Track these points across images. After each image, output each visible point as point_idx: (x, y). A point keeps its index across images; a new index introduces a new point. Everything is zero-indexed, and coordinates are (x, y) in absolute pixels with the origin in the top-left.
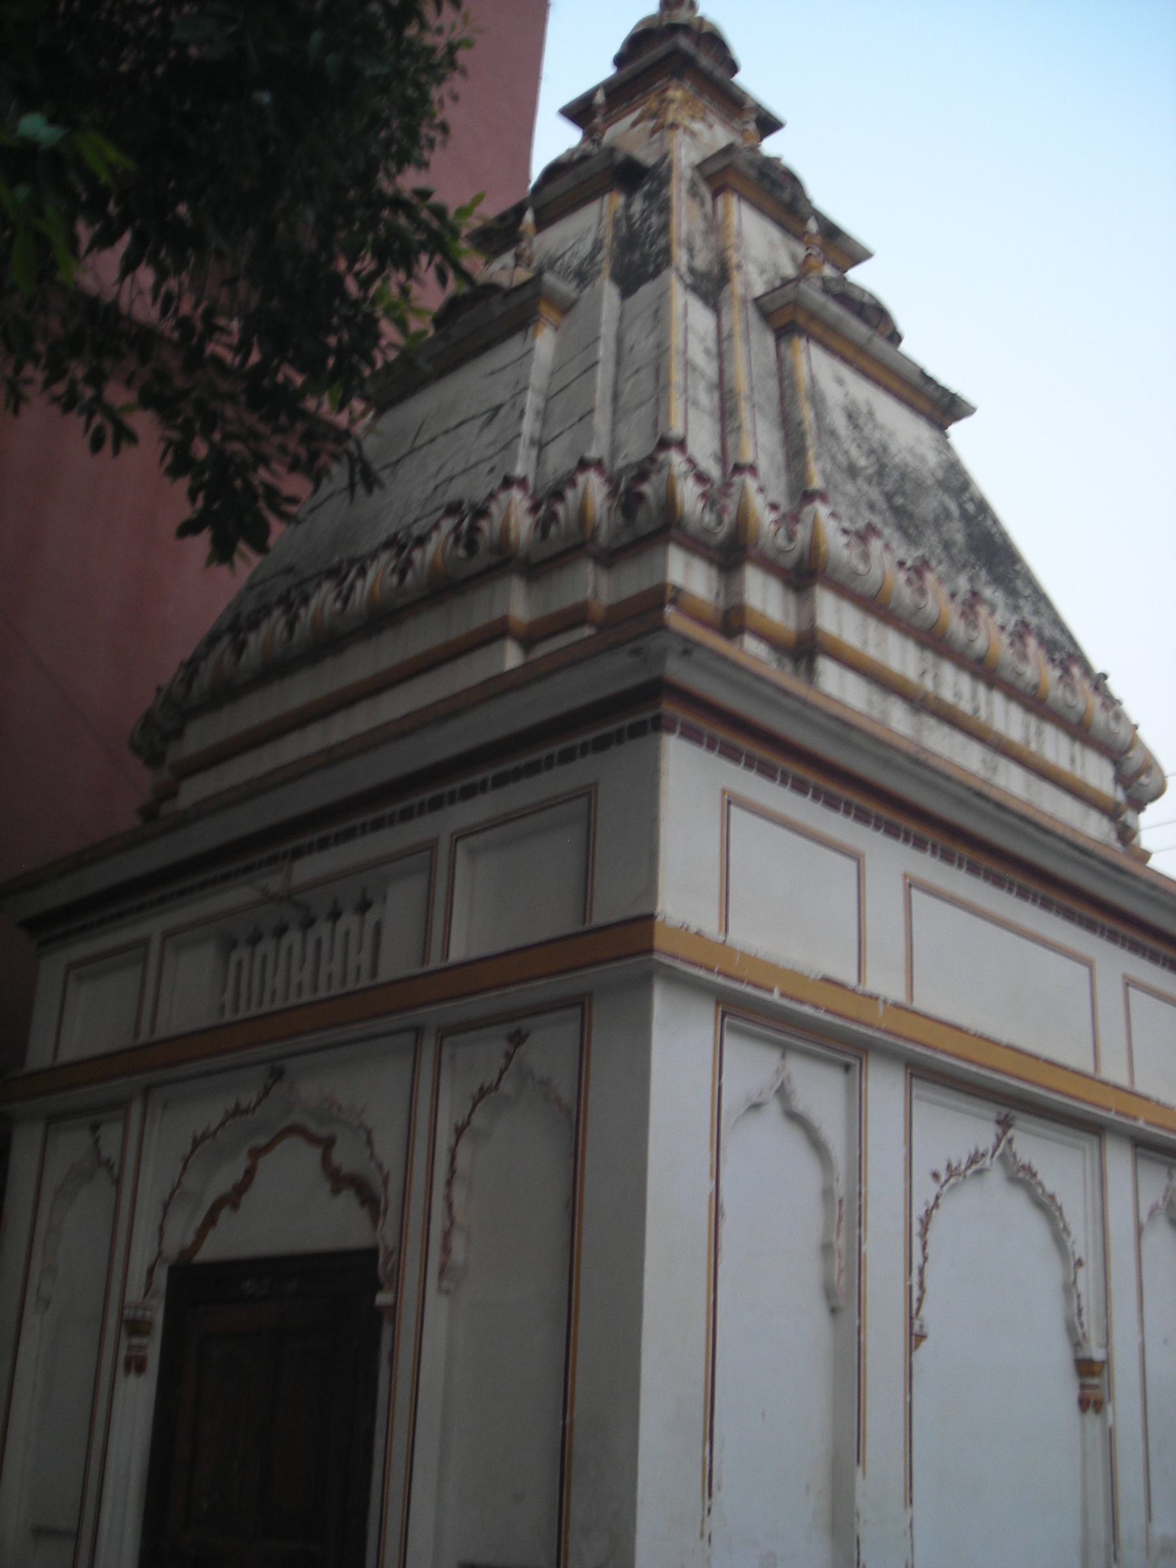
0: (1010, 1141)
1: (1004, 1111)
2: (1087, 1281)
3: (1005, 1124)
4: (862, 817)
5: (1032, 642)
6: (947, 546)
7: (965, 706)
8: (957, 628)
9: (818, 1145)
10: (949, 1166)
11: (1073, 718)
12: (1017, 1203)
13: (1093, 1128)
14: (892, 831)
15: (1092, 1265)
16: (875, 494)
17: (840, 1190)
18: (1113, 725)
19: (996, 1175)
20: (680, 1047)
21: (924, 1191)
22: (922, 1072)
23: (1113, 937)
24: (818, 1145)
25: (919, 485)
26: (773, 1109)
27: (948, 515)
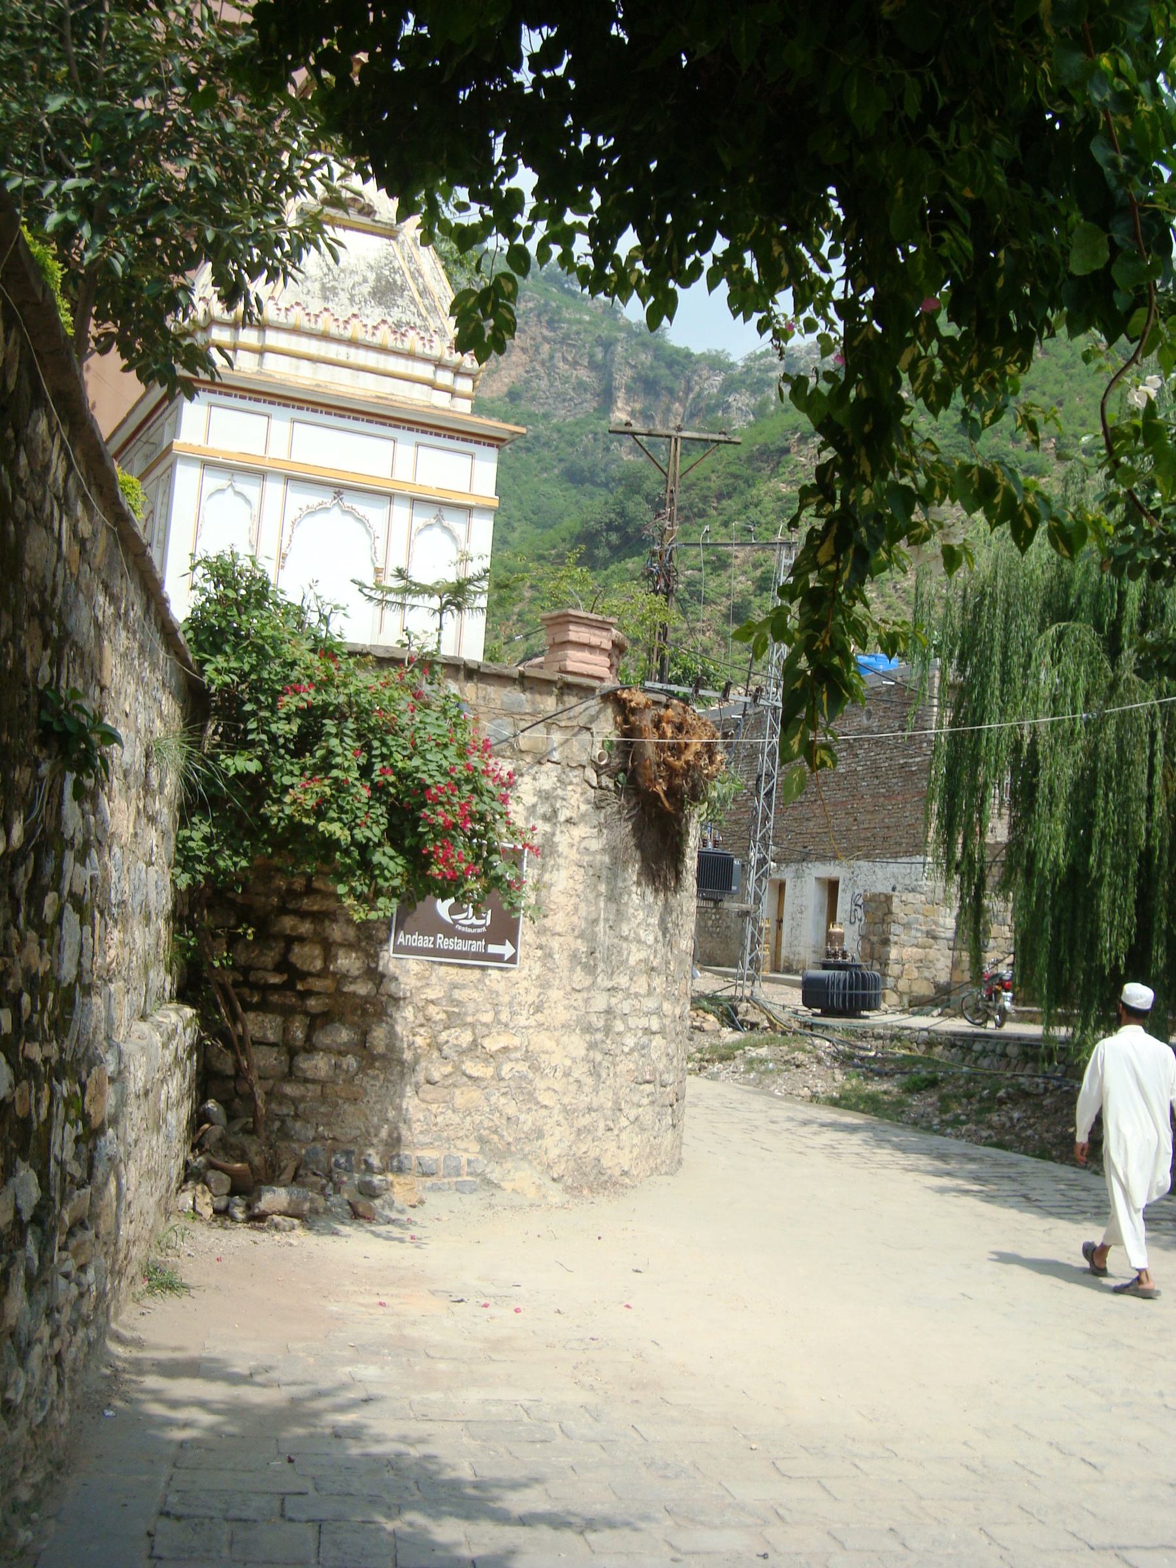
2: (380, 545)
3: (338, 494)
4: (271, 403)
5: (384, 328)
6: (352, 299)
7: (342, 358)
8: (334, 330)
9: (248, 501)
12: (349, 519)
13: (390, 496)
14: (285, 405)
15: (383, 538)
16: (317, 286)
17: (256, 512)
18: (427, 351)
19: (336, 511)
20: (186, 478)
21: (292, 513)
22: (288, 478)
24: (248, 501)
25: (352, 272)
26: (230, 491)
27: (365, 280)
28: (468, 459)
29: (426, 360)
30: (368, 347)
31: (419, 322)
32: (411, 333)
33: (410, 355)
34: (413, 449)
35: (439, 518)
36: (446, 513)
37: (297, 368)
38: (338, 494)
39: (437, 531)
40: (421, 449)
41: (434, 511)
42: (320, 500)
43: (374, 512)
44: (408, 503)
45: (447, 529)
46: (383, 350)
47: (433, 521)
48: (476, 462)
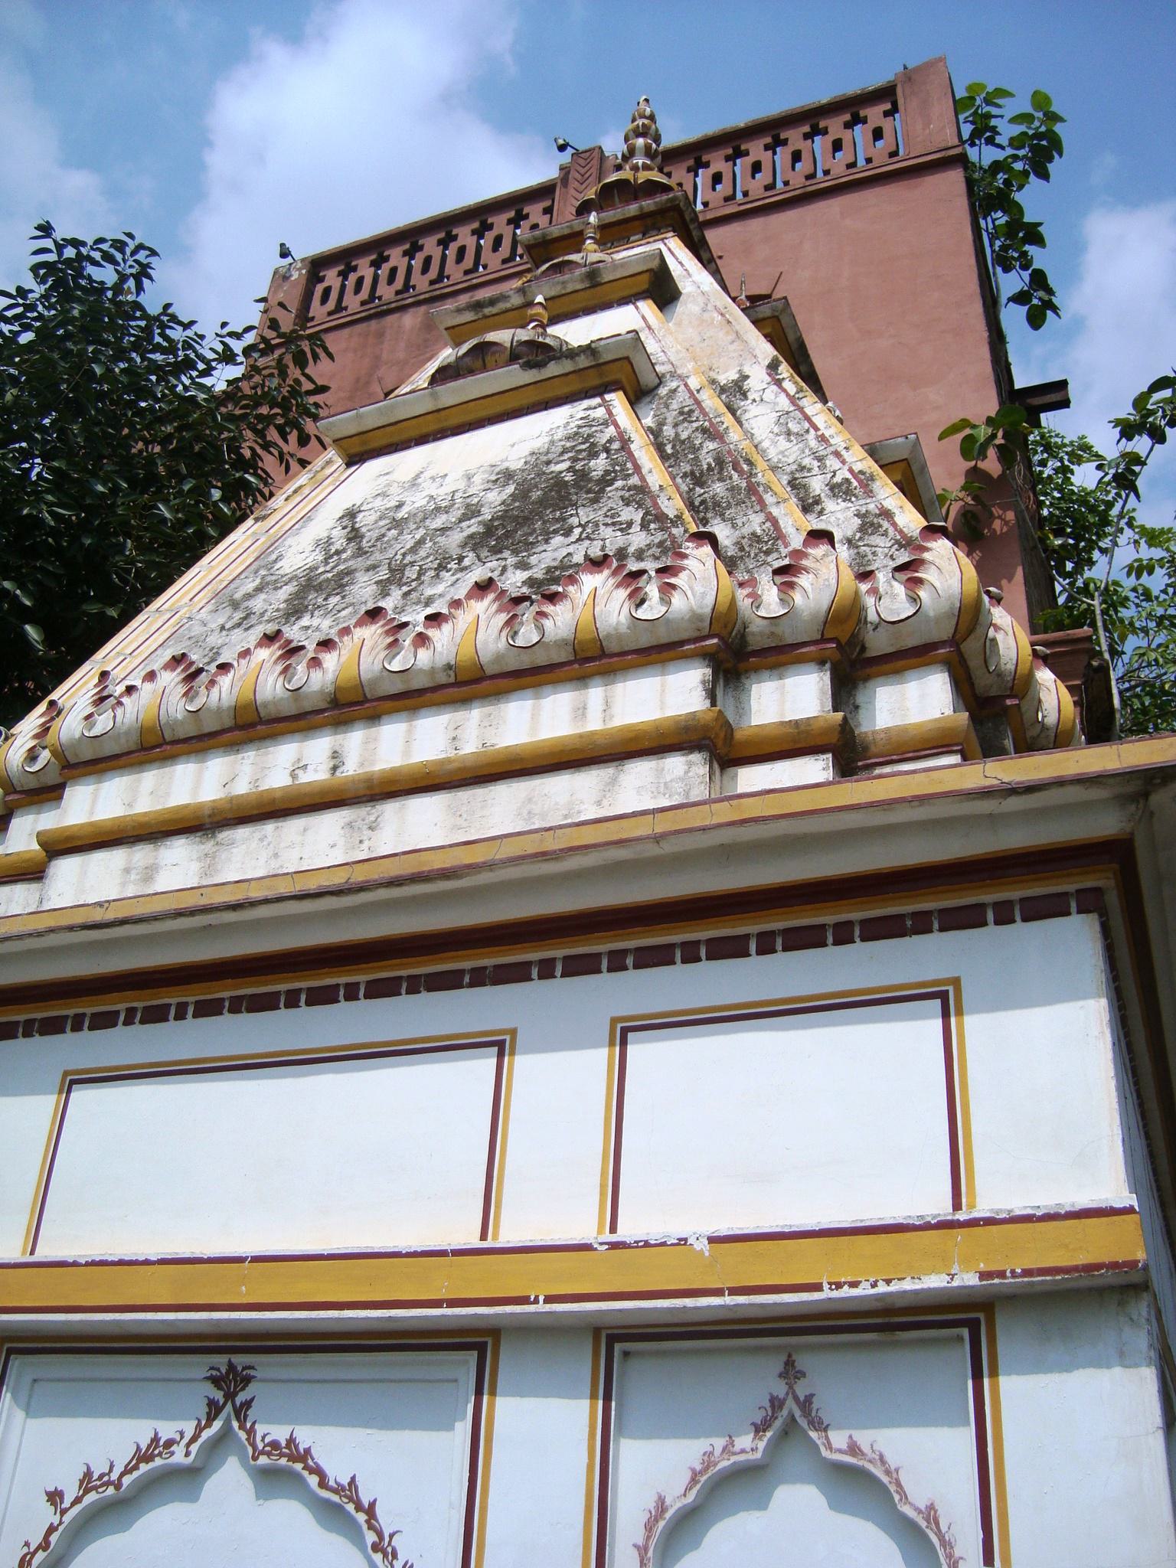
0: (241, 1412)
1: (221, 1361)
3: (231, 1385)
7: (317, 774)
10: (88, 1474)
11: (563, 656)
23: (582, 966)
28: (923, 1030)
29: (656, 651)
30: (411, 698)
31: (638, 539)
32: (591, 581)
33: (591, 660)
34: (597, 1059)
35: (790, 1424)
36: (829, 1377)
37: (149, 873)
38: (231, 1385)
39: (798, 1502)
40: (642, 1052)
41: (755, 1381)
42: (138, 1431)
43: (397, 1459)
44: (582, 1365)
45: (860, 1486)
46: (470, 684)
47: (749, 1446)
48: (975, 1026)
